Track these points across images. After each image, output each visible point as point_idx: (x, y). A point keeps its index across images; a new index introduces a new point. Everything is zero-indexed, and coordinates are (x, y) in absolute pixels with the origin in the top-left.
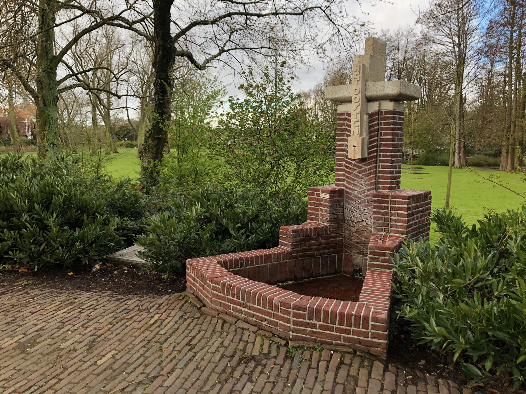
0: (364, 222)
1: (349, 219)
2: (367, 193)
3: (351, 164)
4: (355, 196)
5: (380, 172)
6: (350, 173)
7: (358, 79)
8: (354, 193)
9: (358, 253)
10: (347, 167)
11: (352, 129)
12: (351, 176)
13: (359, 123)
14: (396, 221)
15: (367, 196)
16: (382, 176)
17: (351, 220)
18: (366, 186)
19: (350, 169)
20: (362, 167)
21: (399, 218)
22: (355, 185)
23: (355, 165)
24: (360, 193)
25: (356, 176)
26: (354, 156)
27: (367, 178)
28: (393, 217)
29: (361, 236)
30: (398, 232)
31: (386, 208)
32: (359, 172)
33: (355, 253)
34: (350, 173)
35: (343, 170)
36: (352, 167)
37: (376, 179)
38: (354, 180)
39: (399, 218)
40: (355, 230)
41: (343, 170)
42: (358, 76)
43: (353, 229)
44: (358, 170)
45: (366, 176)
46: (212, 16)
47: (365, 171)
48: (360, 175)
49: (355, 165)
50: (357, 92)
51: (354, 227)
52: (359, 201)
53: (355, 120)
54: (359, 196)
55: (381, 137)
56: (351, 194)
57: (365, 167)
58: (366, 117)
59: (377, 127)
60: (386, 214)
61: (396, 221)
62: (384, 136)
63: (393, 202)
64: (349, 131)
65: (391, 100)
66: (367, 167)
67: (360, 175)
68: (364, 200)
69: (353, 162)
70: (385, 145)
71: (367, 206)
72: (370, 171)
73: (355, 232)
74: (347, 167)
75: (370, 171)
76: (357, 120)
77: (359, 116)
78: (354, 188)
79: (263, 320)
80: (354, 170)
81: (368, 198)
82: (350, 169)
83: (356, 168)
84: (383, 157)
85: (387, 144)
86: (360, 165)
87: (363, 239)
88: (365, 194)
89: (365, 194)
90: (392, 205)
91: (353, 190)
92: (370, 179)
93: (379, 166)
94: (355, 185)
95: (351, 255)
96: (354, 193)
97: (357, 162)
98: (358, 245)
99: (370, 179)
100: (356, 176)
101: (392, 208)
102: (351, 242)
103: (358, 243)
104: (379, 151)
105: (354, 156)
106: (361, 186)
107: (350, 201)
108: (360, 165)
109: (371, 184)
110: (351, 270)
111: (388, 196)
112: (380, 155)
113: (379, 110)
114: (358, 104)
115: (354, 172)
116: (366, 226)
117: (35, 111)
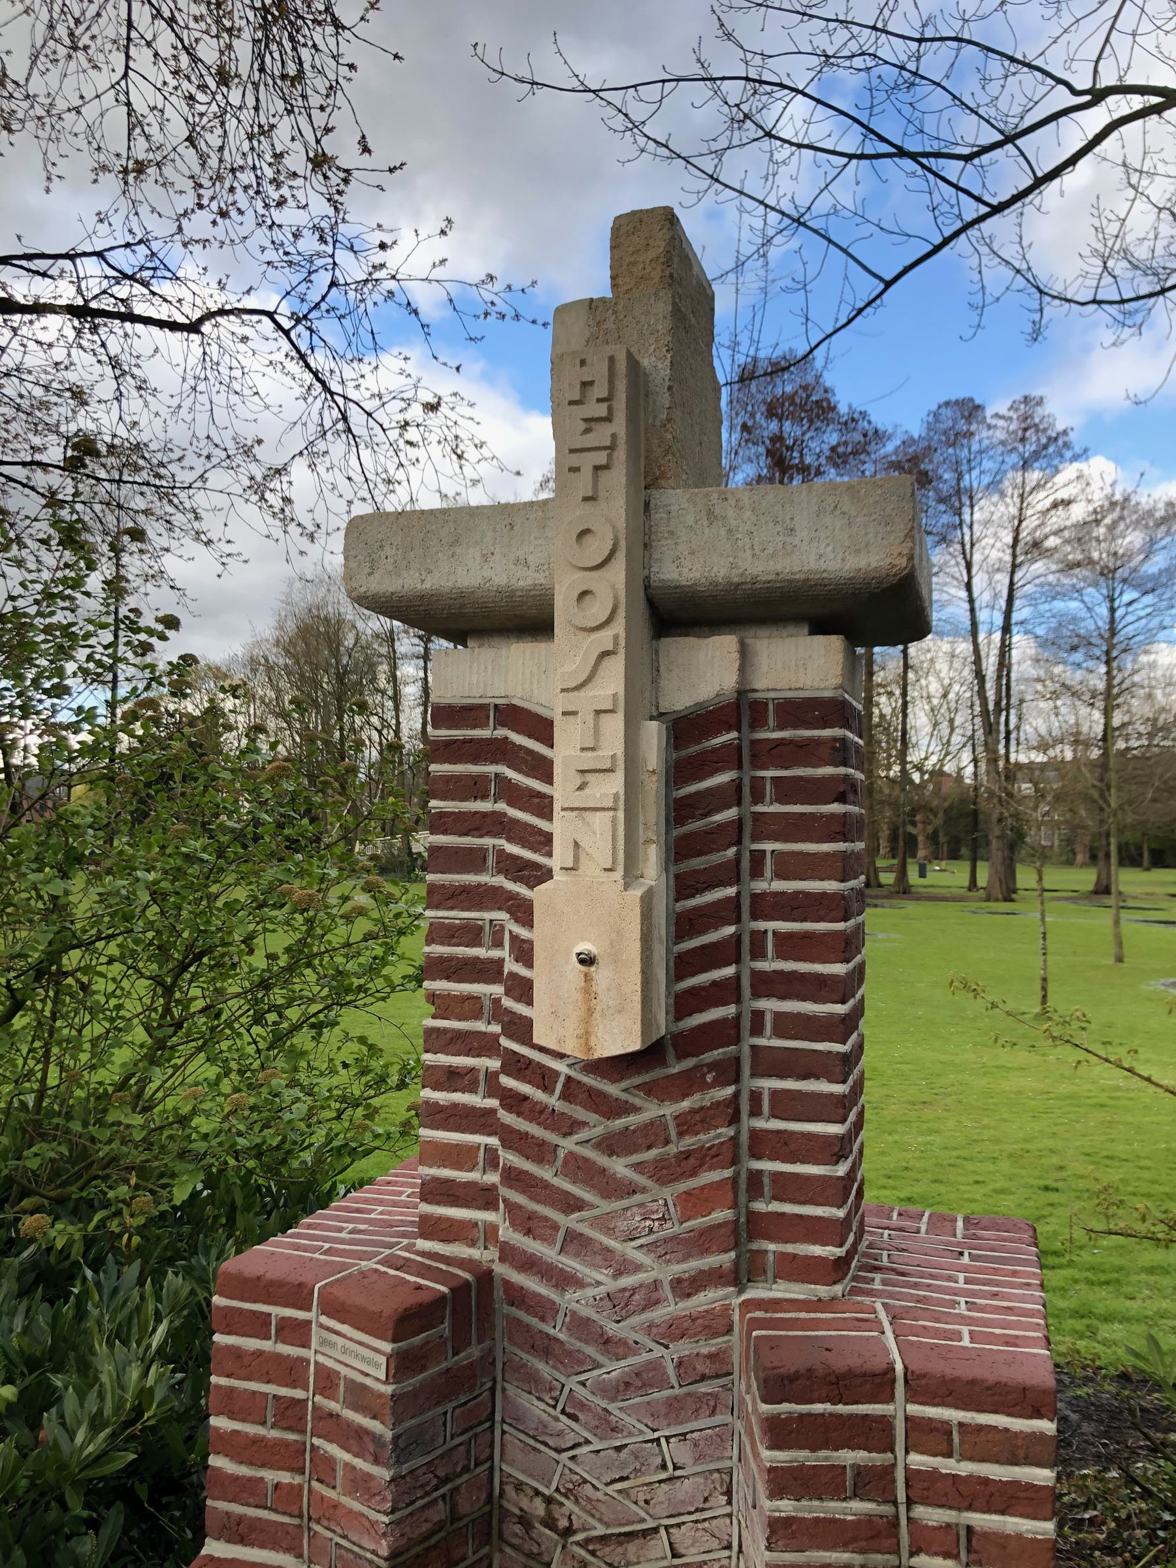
2: (671, 1308)
4: (580, 1325)
5: (762, 1144)
6: (541, 1152)
7: (601, 458)
8: (570, 1300)
10: (515, 1102)
11: (560, 827)
12: (545, 1173)
13: (615, 784)
15: (674, 1331)
16: (777, 1176)
17: (549, 1522)
18: (665, 1249)
19: (537, 1113)
20: (627, 1109)
22: (574, 1242)
24: (619, 1303)
25: (578, 1168)
26: (586, 1036)
27: (668, 1193)
32: (611, 1145)
34: (541, 1152)
35: (480, 1121)
36: (553, 1101)
37: (735, 1205)
38: (571, 1205)
41: (480, 1121)
42: (601, 434)
44: (598, 1126)
45: (663, 1172)
47: (653, 1133)
48: (620, 1167)
50: (597, 548)
52: (615, 1369)
53: (588, 761)
54: (612, 1329)
55: (760, 886)
56: (545, 1310)
57: (651, 1111)
58: (653, 734)
59: (731, 813)
62: (780, 875)
64: (544, 842)
65: (820, 627)
66: (669, 1110)
67: (620, 1167)
68: (655, 1366)
70: (789, 946)
71: (674, 1409)
72: (689, 1142)
74: (515, 1102)
75: (689, 1142)
76: (602, 757)
77: (615, 726)
78: (569, 1263)
80: (571, 1127)
81: (684, 1348)
82: (537, 1113)
83: (579, 1113)
84: (778, 1033)
85: (807, 936)
86: (613, 1089)
88: (658, 1314)
89: (658, 1314)
90: (919, 1461)
91: (565, 1280)
93: (756, 1097)
94: (574, 1242)
96: (570, 1300)
99: (693, 1203)
100: (578, 1168)
104: (746, 982)
105: (586, 1036)
106: (630, 1251)
107: (543, 1368)
108: (613, 1089)
109: (702, 1242)
112: (758, 1016)
113: (741, 693)
114: (604, 639)
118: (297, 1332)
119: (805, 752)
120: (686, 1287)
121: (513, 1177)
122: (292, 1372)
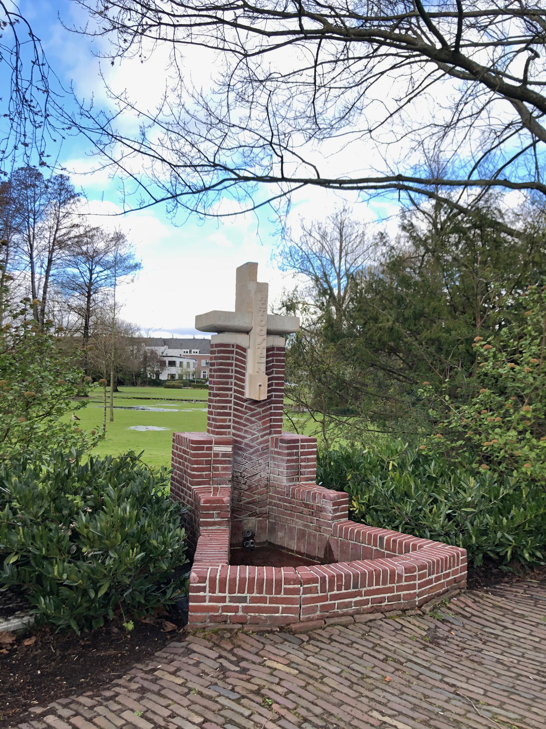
0: (258, 476)
1: (239, 474)
2: (261, 440)
3: (242, 406)
4: (246, 445)
5: (272, 414)
6: (241, 418)
8: (245, 441)
9: (250, 516)
12: (242, 421)
14: (305, 467)
15: (261, 443)
17: (241, 476)
18: (259, 431)
20: (255, 410)
21: (309, 463)
22: (246, 432)
23: (246, 408)
24: (252, 440)
25: (247, 420)
26: (259, 397)
27: (260, 422)
28: (303, 464)
29: (254, 494)
30: (307, 479)
31: (297, 454)
32: (252, 416)
33: (246, 517)
34: (241, 418)
38: (245, 426)
39: (309, 463)
40: (247, 487)
43: (244, 487)
44: (250, 413)
45: (260, 419)
46: (460, 175)
47: (259, 413)
48: (253, 419)
49: (246, 408)
51: (245, 484)
52: (252, 450)
54: (251, 444)
56: (241, 443)
57: (259, 410)
60: (297, 461)
61: (305, 467)
63: (303, 447)
66: (261, 409)
67: (253, 419)
68: (258, 449)
69: (245, 404)
71: (261, 455)
73: (246, 491)
78: (245, 435)
79: (382, 600)
80: (245, 413)
81: (262, 445)
83: (247, 411)
86: (253, 407)
87: (256, 496)
88: (258, 441)
89: (258, 441)
90: (302, 450)
91: (244, 438)
92: (264, 423)
94: (246, 432)
95: (240, 521)
96: (245, 441)
97: (249, 404)
98: (250, 505)
99: (264, 423)
100: (247, 420)
101: (303, 454)
102: (241, 503)
103: (249, 503)
105: (259, 397)
106: (254, 432)
107: (240, 452)
108: (253, 407)
109: (265, 429)
110: (241, 539)
111: (297, 441)
115: (246, 416)
116: (259, 480)
117: (509, 226)
118: (210, 449)
119: (280, 355)
120: (262, 436)
121: (235, 422)
122: (209, 455)
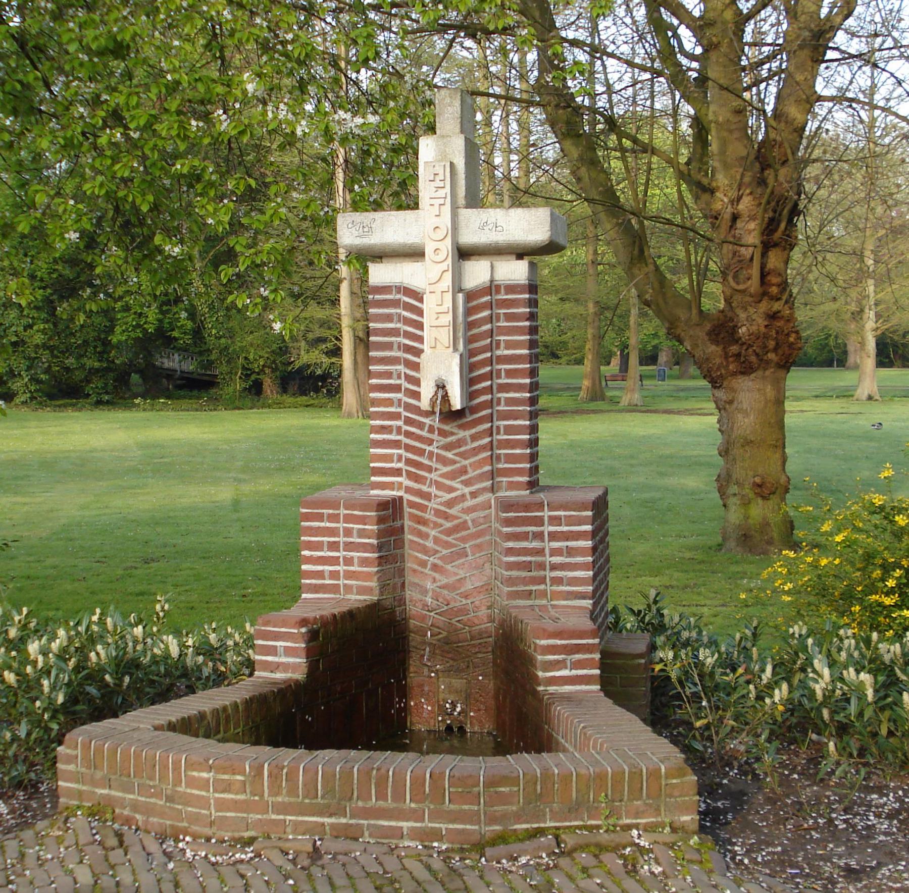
2: (470, 503)
3: (421, 426)
4: (438, 513)
6: (421, 452)
7: (442, 201)
8: (432, 505)
10: (408, 434)
11: (426, 334)
13: (450, 317)
16: (506, 455)
19: (419, 438)
31: (539, 536)
32: (447, 447)
34: (421, 452)
35: (396, 444)
36: (424, 433)
37: (492, 465)
41: (396, 444)
42: (441, 193)
48: (449, 455)
50: (440, 234)
53: (440, 309)
55: (499, 353)
57: (462, 434)
58: (460, 296)
59: (488, 326)
62: (507, 348)
64: (420, 339)
65: (520, 256)
67: (449, 455)
70: (510, 373)
72: (476, 444)
74: (408, 434)
75: (476, 444)
76: (443, 309)
77: (449, 297)
81: (474, 515)
82: (419, 438)
84: (507, 405)
85: (516, 370)
93: (498, 428)
101: (553, 536)
104: (495, 387)
112: (499, 399)
113: (492, 281)
114: (444, 266)
120: (474, 495)
121: (409, 462)
